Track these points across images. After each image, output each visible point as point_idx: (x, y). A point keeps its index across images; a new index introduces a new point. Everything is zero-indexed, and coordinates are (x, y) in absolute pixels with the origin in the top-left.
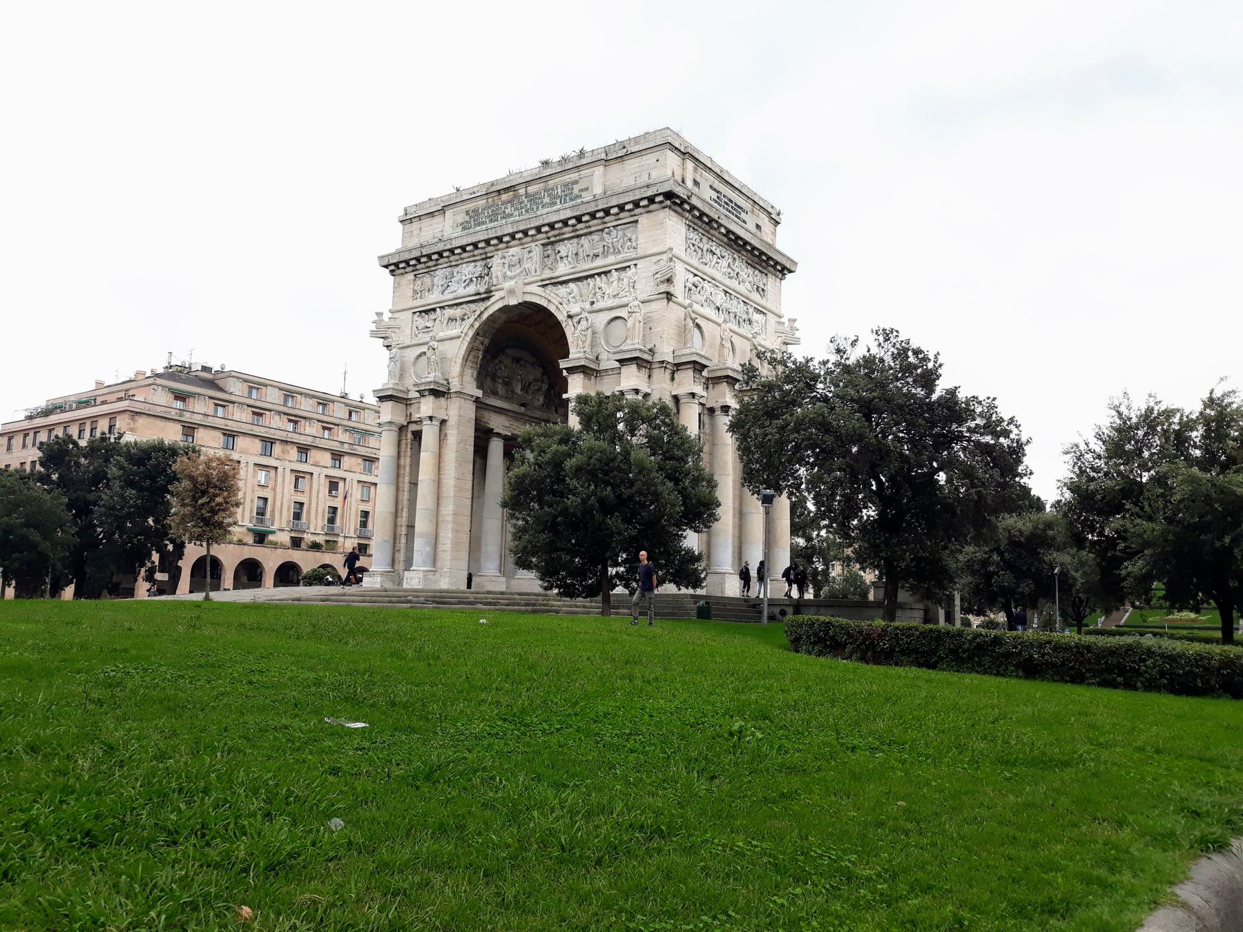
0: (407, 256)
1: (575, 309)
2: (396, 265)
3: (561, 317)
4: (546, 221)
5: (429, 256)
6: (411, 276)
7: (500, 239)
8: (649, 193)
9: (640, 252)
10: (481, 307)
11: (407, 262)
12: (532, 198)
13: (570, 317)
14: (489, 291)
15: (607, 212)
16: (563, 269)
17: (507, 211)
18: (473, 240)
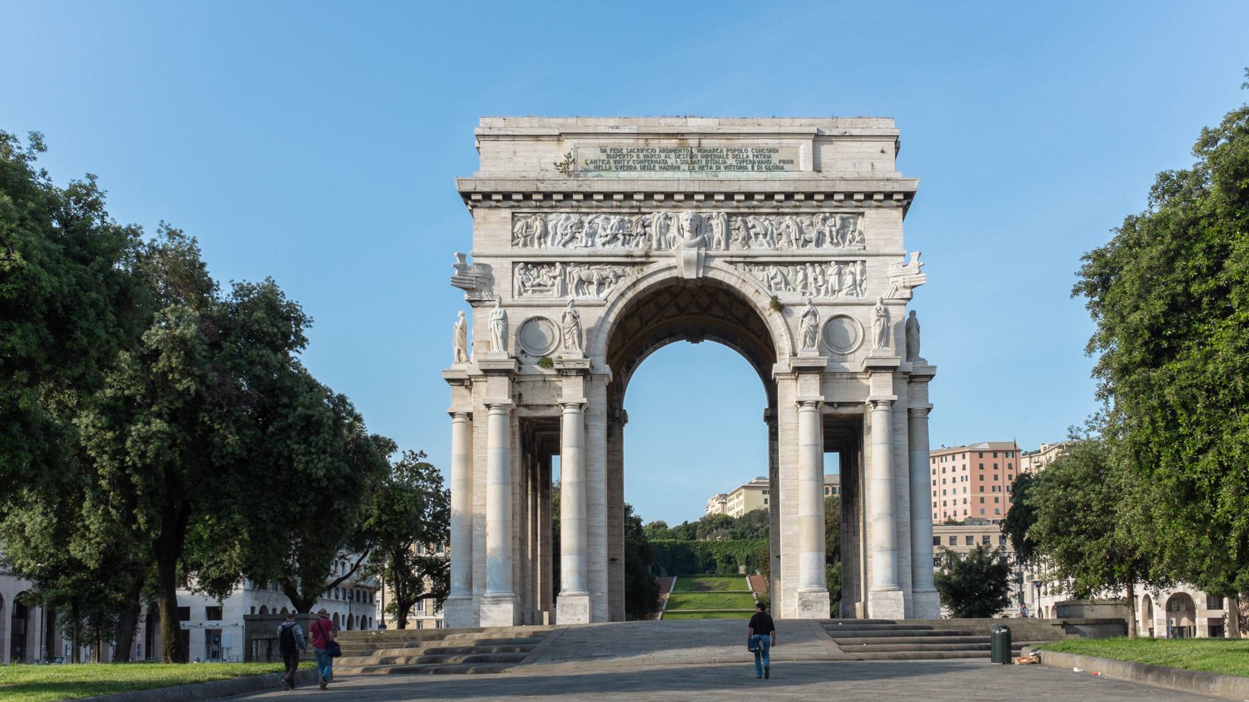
0: (508, 187)
1: (785, 297)
2: (487, 196)
3: (762, 303)
4: (744, 189)
5: (548, 196)
6: (507, 213)
7: (669, 196)
8: (888, 189)
9: (869, 250)
10: (632, 274)
11: (507, 196)
12: (710, 154)
13: (779, 306)
14: (647, 255)
15: (829, 196)
16: (760, 248)
17: (670, 162)
18: (628, 188)
